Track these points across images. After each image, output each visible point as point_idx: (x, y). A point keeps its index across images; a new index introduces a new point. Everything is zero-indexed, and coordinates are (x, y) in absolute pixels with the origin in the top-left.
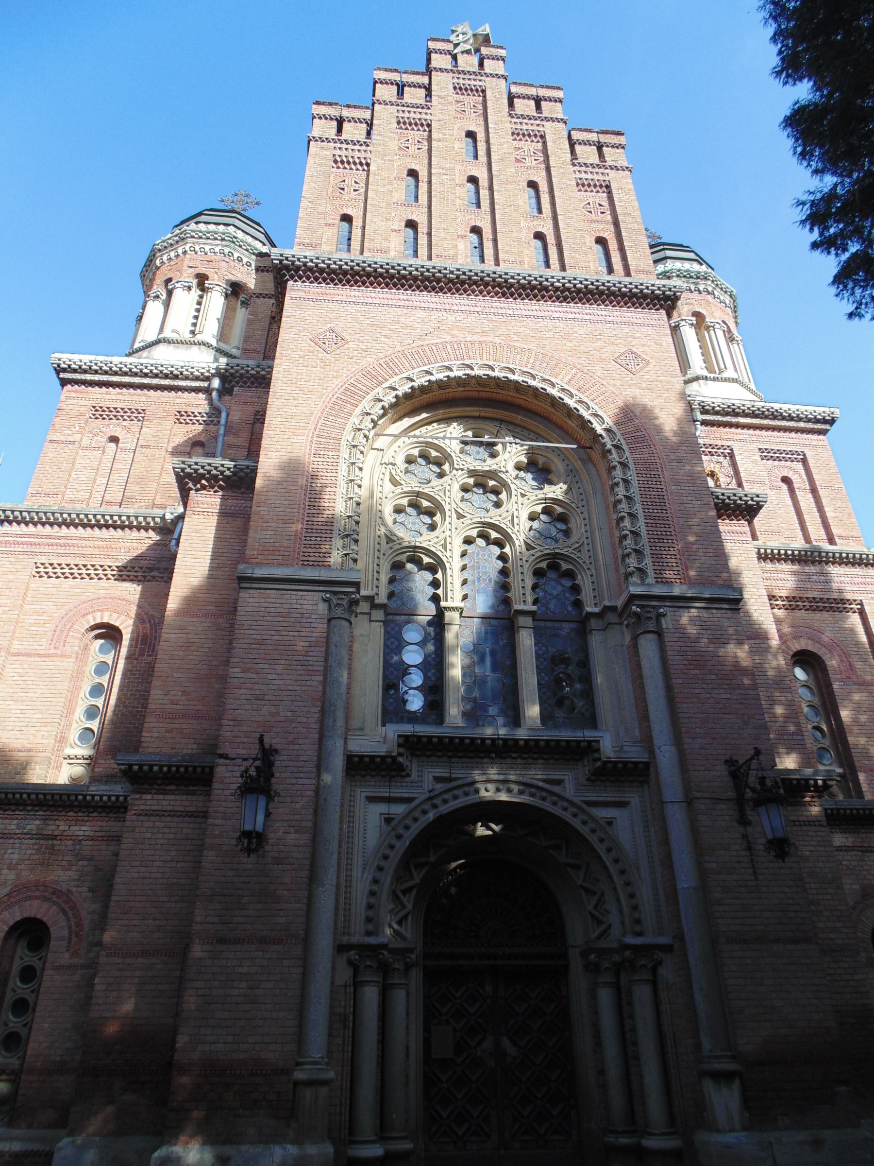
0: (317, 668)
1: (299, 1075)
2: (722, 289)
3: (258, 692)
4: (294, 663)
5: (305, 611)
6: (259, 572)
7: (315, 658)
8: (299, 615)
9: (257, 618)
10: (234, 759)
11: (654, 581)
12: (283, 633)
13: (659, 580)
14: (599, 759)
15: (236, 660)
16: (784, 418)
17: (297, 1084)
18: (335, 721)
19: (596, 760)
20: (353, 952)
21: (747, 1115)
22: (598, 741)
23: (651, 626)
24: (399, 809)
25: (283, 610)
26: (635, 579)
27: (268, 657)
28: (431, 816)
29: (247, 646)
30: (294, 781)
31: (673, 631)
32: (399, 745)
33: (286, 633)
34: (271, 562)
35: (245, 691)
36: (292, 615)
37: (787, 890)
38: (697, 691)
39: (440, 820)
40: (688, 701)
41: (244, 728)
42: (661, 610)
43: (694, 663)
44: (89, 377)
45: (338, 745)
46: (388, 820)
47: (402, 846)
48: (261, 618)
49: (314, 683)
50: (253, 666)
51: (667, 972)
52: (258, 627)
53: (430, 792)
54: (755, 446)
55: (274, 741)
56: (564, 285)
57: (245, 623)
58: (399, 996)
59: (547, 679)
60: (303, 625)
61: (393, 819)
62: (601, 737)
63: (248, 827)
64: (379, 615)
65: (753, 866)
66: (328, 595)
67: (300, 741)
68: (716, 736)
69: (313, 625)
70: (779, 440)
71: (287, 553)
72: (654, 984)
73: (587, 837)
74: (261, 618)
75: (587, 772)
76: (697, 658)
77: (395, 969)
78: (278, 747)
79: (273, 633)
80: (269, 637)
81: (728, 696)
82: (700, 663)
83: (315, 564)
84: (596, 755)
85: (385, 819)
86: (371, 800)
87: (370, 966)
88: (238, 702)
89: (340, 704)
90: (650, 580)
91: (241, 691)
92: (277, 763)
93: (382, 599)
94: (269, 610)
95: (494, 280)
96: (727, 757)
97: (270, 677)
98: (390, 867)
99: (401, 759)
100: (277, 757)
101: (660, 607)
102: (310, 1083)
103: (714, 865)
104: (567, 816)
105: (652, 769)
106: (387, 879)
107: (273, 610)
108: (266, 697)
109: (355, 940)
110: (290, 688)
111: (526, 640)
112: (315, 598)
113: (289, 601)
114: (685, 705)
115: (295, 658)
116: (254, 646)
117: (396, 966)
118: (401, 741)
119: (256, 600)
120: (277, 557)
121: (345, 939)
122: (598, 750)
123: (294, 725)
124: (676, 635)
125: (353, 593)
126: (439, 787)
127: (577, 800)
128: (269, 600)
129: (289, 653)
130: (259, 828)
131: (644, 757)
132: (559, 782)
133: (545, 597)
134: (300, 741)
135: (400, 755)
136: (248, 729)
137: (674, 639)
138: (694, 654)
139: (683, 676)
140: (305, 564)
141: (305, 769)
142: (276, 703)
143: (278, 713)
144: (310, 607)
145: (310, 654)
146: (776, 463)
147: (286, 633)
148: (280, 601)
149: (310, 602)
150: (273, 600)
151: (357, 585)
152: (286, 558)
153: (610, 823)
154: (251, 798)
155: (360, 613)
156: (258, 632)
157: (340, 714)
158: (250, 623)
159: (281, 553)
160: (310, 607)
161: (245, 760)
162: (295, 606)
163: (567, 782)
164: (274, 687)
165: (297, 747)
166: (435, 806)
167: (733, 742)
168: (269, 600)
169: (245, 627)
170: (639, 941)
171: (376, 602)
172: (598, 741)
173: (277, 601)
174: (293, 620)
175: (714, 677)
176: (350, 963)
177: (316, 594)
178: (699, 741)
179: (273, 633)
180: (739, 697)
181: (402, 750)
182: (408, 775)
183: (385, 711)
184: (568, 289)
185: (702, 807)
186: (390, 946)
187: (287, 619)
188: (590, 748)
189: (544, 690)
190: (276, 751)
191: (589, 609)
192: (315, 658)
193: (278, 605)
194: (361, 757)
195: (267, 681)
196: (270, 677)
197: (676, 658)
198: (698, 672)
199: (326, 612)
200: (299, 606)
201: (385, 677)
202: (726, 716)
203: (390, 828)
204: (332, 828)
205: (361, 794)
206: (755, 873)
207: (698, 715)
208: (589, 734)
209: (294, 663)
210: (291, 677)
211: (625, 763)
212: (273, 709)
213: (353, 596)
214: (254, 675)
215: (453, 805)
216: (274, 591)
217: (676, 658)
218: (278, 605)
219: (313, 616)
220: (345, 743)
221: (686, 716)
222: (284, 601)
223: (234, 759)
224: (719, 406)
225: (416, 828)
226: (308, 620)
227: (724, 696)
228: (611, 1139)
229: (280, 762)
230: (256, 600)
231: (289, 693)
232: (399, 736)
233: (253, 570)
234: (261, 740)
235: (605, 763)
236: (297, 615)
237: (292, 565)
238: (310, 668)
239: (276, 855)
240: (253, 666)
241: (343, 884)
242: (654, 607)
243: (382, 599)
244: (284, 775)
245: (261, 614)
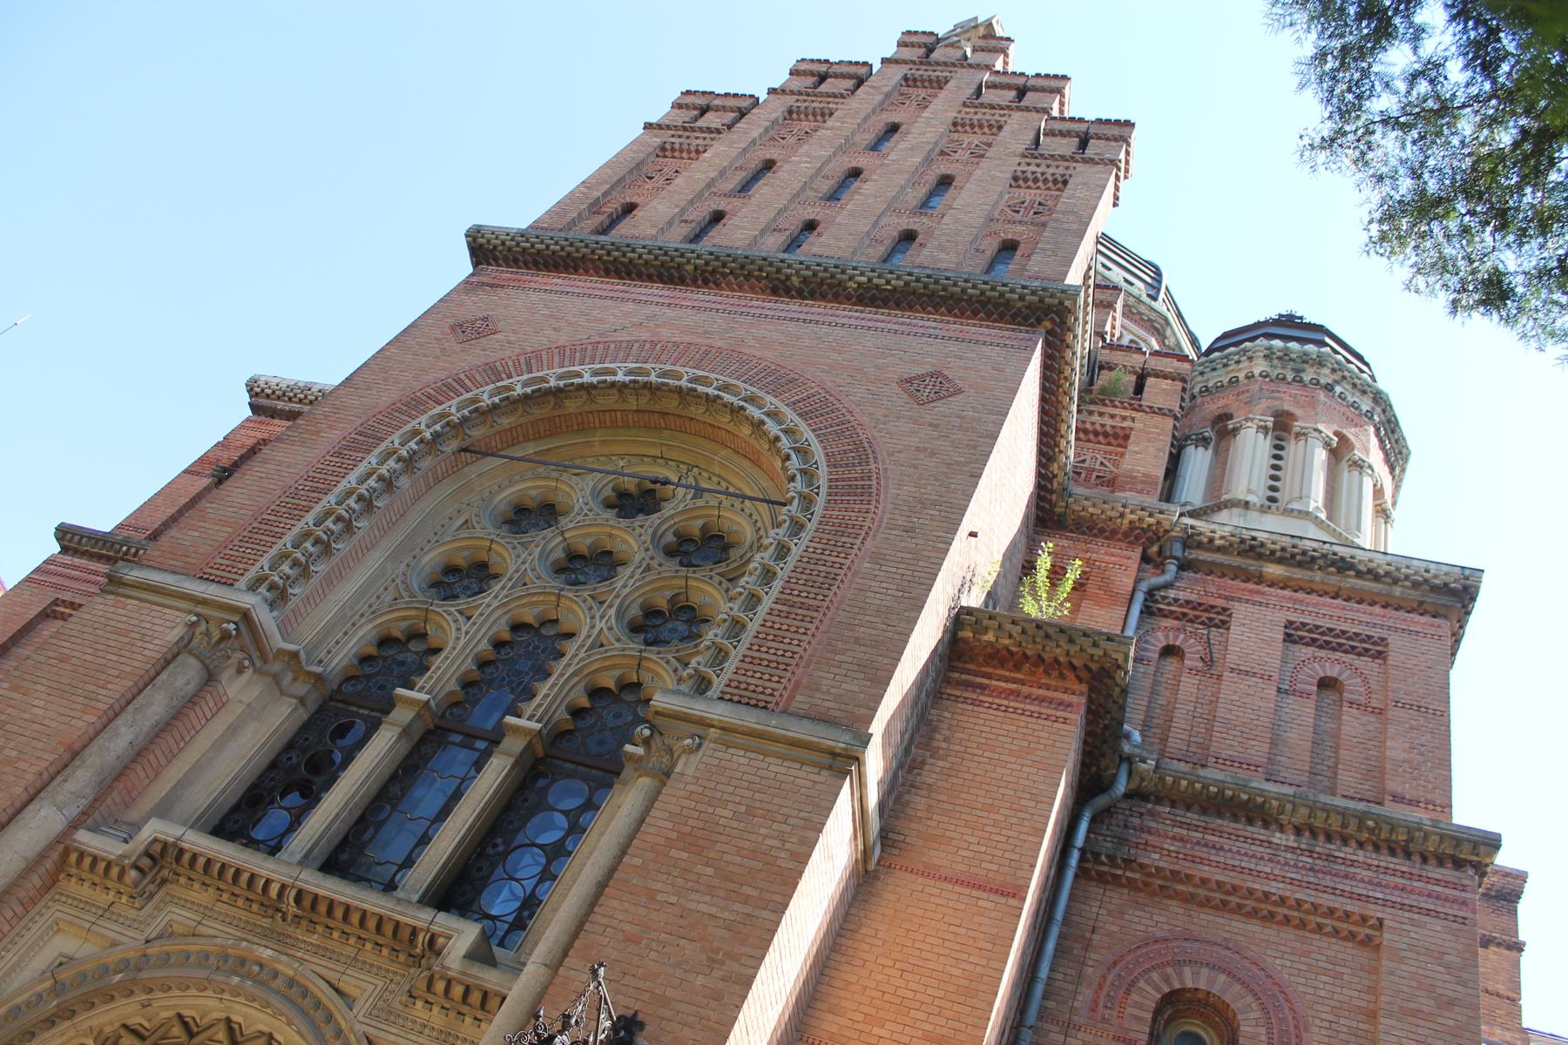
0: (100, 705)
2: (1354, 386)
16: (1359, 574)
44: (280, 405)
54: (1282, 617)
56: (870, 280)
62: (456, 931)
70: (1338, 613)
81: (713, 910)
95: (760, 270)
96: (629, 1013)
146: (1322, 653)
172: (449, 938)
181: (146, 862)
184: (877, 287)
224: (1222, 538)
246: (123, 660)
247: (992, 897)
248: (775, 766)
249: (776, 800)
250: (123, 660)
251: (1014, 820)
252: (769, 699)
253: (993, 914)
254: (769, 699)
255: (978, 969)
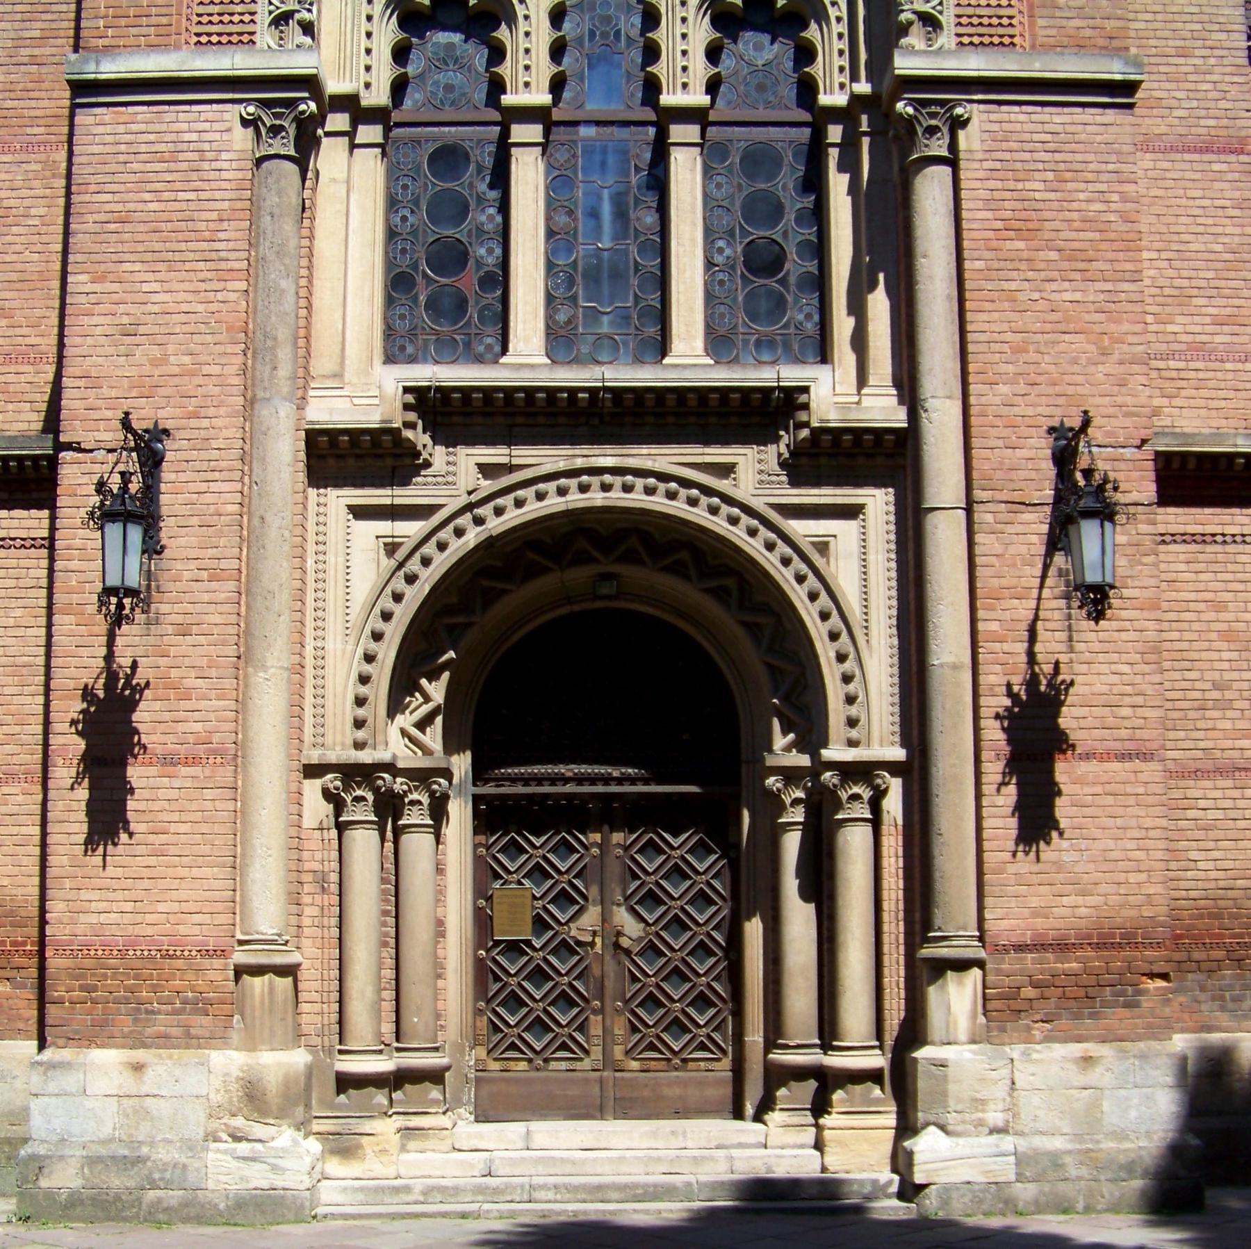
0: (237, 265)
1: (241, 957)
3: (125, 320)
4: (191, 256)
5: (206, 146)
6: (110, 69)
7: (231, 245)
8: (195, 156)
9: (113, 168)
10: (91, 451)
11: (954, 40)
12: (166, 196)
13: (966, 40)
14: (806, 424)
15: (79, 258)
17: (240, 971)
18: (275, 368)
19: (800, 425)
20: (330, 776)
21: (982, 1019)
22: (806, 390)
23: (938, 147)
24: (411, 529)
25: (162, 147)
26: (915, 39)
27: (140, 248)
28: (473, 537)
29: (98, 228)
30: (203, 487)
31: (980, 156)
32: (407, 407)
33: (172, 196)
34: (132, 41)
35: (101, 320)
36: (181, 156)
37: (1126, 669)
38: (1013, 285)
39: (489, 545)
40: (988, 306)
41: (105, 391)
42: (959, 111)
43: (1018, 225)
45: (282, 414)
46: (391, 549)
47: (415, 595)
48: (121, 168)
49: (233, 296)
50: (111, 267)
51: (893, 804)
52: (115, 187)
53: (470, 493)
55: (161, 414)
57: (92, 179)
58: (418, 845)
59: (728, 252)
60: (205, 176)
61: (401, 544)
62: (814, 380)
63: (113, 580)
64: (370, 133)
65: (1070, 627)
66: (251, 109)
67: (211, 412)
68: (1039, 379)
69: (225, 175)
71: (164, 20)
72: (876, 822)
73: (772, 571)
74: (121, 168)
75: (783, 449)
76: (1024, 215)
77: (412, 803)
78: (169, 425)
79: (147, 196)
80: (140, 206)
81: (1078, 296)
82: (1030, 225)
83: (224, 39)
84: (802, 416)
85: (385, 544)
86: (360, 512)
87: (363, 799)
88: (89, 340)
89: (283, 333)
90: (946, 39)
91: (96, 320)
92: (169, 456)
93: (378, 96)
94: (134, 149)
96: (1055, 423)
97: (146, 287)
98: (395, 632)
99: (408, 434)
100: (168, 444)
101: (959, 103)
102: (258, 970)
103: (994, 626)
104: (737, 535)
105: (910, 443)
106: (388, 653)
107: (143, 148)
108: (142, 329)
109: (333, 757)
110: (185, 307)
111: (686, 171)
112: (227, 116)
113: (175, 127)
114: (984, 317)
115: (191, 245)
116: (112, 227)
117: (415, 796)
118: (410, 398)
119: (109, 129)
120: (144, 31)
121: (314, 757)
122: (806, 407)
123: (199, 380)
124: (987, 165)
125: (303, 100)
126: (488, 486)
127: (758, 504)
128: (134, 127)
129: (180, 236)
130: (134, 579)
131: (898, 418)
132: (726, 470)
133: (736, 73)
134: (211, 412)
135: (410, 425)
136: (114, 393)
137: (981, 174)
138: (1019, 205)
139: (988, 255)
140: (204, 43)
141: (223, 464)
142: (159, 339)
143: (164, 360)
144: (217, 136)
145: (222, 235)
147: (172, 196)
148: (157, 127)
149: (216, 126)
150: (143, 127)
151: (310, 83)
152: (162, 30)
153: (823, 548)
154: (113, 530)
155: (328, 134)
156: (117, 197)
157: (284, 354)
158: (100, 178)
159: (154, 20)
160: (217, 136)
161: (110, 451)
162: (187, 137)
163: (740, 469)
164: (156, 308)
165: (205, 423)
166: (479, 521)
167: (1071, 390)
168: (134, 127)
169: (93, 188)
170: (850, 755)
171: (364, 103)
172: (806, 390)
173: (151, 127)
174: (184, 166)
175: (1053, 255)
176: (327, 794)
177: (229, 106)
178: (1004, 389)
179: (147, 196)
180: (1102, 297)
181: (412, 416)
182: (427, 464)
183: (389, 333)
185: (989, 518)
186: (400, 765)
187: (172, 166)
188: (789, 402)
189: (721, 276)
190: (166, 432)
191: (824, 99)
192: (231, 245)
193: (152, 137)
194: (333, 435)
195: (141, 297)
196: (146, 287)
197: (981, 215)
198: (1021, 245)
199: (249, 145)
200: (194, 137)
201: (389, 263)
202: (1066, 337)
203: (393, 563)
204: (277, 570)
205: (339, 499)
206: (1070, 639)
207: (1009, 336)
208: (791, 374)
209: (191, 256)
210: (186, 286)
211: (858, 433)
212: (156, 352)
213: (302, 107)
214: (115, 287)
215: (514, 517)
216: (145, 108)
217: (981, 215)
218: (152, 137)
219: (224, 156)
220: (300, 408)
221: (983, 337)
222: (164, 127)
223: (91, 451)
225: (442, 562)
226: (215, 165)
227: (1068, 296)
228: (778, 1056)
229: (173, 452)
230: (109, 129)
231: (184, 318)
232: (407, 390)
233: (98, 63)
234: (126, 424)
235: (817, 433)
236: (191, 156)
237: (177, 47)
238: (223, 265)
239: (179, 619)
240: (111, 267)
241: (309, 662)
242: (942, 103)
243: (378, 96)
244: (183, 477)
245: (122, 158)
246: (203, 195)
247: (1223, 157)
248: (1058, 118)
249: (1079, 157)
250: (203, 195)
251: (1212, 61)
252: (1010, 31)
253: (1230, 177)
254: (1010, 31)
255: (1237, 240)
